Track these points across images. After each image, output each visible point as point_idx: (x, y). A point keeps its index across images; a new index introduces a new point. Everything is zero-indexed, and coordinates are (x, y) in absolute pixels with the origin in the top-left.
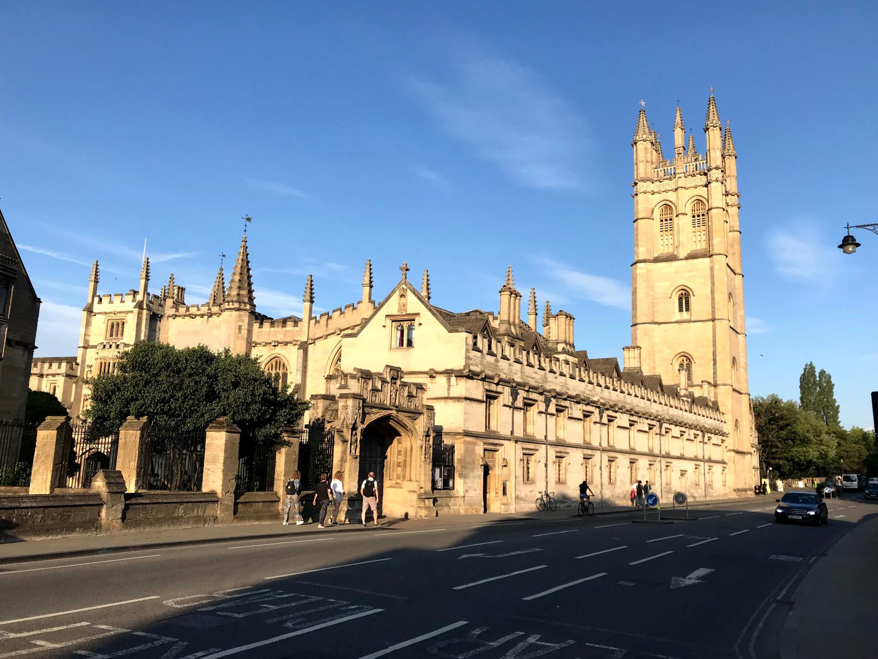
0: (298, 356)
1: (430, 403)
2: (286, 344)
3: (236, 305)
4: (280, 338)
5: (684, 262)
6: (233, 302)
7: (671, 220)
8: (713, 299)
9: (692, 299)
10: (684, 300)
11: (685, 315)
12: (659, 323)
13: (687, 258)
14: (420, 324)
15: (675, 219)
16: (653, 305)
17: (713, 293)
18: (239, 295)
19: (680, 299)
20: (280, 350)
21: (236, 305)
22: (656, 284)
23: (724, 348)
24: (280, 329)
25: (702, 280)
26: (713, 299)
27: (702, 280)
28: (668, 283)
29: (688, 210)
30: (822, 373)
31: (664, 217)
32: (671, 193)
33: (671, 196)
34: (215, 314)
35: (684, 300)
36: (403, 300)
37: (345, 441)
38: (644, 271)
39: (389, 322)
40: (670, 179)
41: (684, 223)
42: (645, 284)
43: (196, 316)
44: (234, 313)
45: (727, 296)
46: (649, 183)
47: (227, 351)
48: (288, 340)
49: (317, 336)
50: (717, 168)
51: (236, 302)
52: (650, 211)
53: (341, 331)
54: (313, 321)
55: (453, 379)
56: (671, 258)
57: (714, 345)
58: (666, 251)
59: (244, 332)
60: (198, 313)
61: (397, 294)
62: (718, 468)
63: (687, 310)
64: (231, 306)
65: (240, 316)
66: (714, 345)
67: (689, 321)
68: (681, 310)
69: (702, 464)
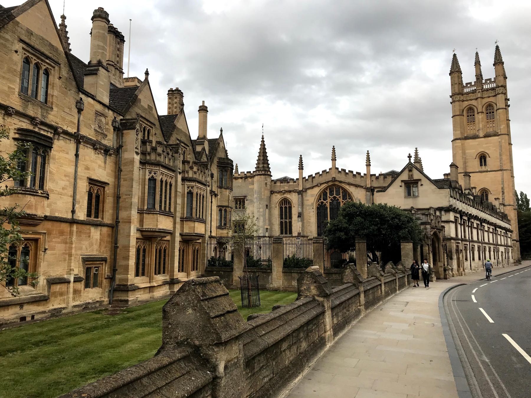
0: (299, 198)
1: (443, 224)
2: (290, 192)
3: (263, 172)
4: (286, 188)
5: (483, 139)
6: (261, 170)
7: (474, 115)
8: (501, 159)
10: (483, 158)
11: (484, 168)
14: (422, 185)
16: (465, 163)
17: (500, 155)
18: (263, 167)
20: (288, 196)
21: (263, 172)
22: (467, 151)
23: (509, 185)
24: (286, 184)
25: (495, 148)
26: (501, 159)
27: (495, 148)
28: (474, 151)
29: (484, 110)
30: (522, 194)
31: (469, 114)
32: (473, 101)
34: (249, 177)
35: (483, 158)
36: (411, 173)
37: (428, 245)
38: (460, 144)
39: (403, 184)
40: (473, 93)
41: (480, 118)
42: (461, 151)
43: (238, 178)
44: (262, 176)
46: (460, 96)
47: (386, 204)
48: (291, 189)
49: (307, 187)
50: (502, 86)
51: (263, 170)
52: (461, 111)
53: (321, 184)
54: (304, 180)
55: (443, 213)
56: (475, 137)
57: (503, 184)
58: (472, 133)
59: (268, 186)
60: (239, 176)
61: (407, 170)
62: (510, 249)
63: (485, 165)
64: (260, 173)
65: (266, 178)
66: (503, 184)
67: (487, 171)
68: (481, 165)
69: (487, 246)
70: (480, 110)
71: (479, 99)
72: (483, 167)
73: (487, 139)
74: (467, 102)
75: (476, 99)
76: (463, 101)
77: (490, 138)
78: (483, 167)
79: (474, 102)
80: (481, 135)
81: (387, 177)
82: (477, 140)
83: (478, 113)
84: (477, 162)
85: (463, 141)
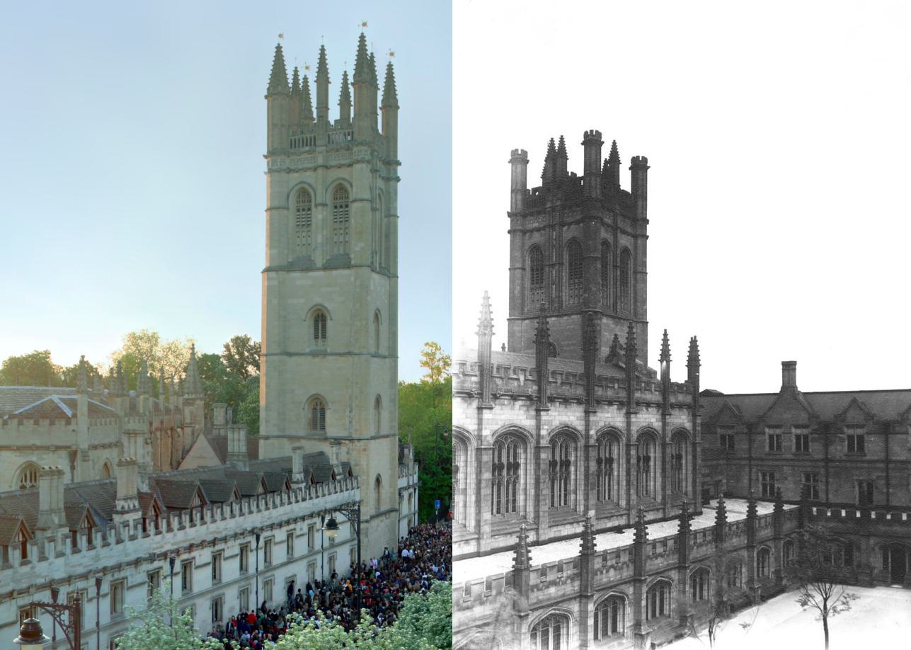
5: (321, 273)
7: (309, 209)
9: (329, 323)
10: (320, 319)
12: (290, 354)
13: (326, 268)
15: (313, 209)
19: (316, 321)
28: (302, 301)
32: (308, 173)
33: (309, 177)
35: (320, 319)
45: (355, 471)
63: (324, 337)
68: (316, 337)
70: (319, 201)
71: (320, 171)
72: (320, 341)
73: (328, 273)
74: (296, 175)
75: (315, 169)
76: (289, 171)
77: (334, 272)
78: (320, 341)
79: (309, 177)
80: (319, 263)
81: (25, 422)
82: (311, 274)
83: (316, 206)
84: (307, 328)
85: (283, 274)
